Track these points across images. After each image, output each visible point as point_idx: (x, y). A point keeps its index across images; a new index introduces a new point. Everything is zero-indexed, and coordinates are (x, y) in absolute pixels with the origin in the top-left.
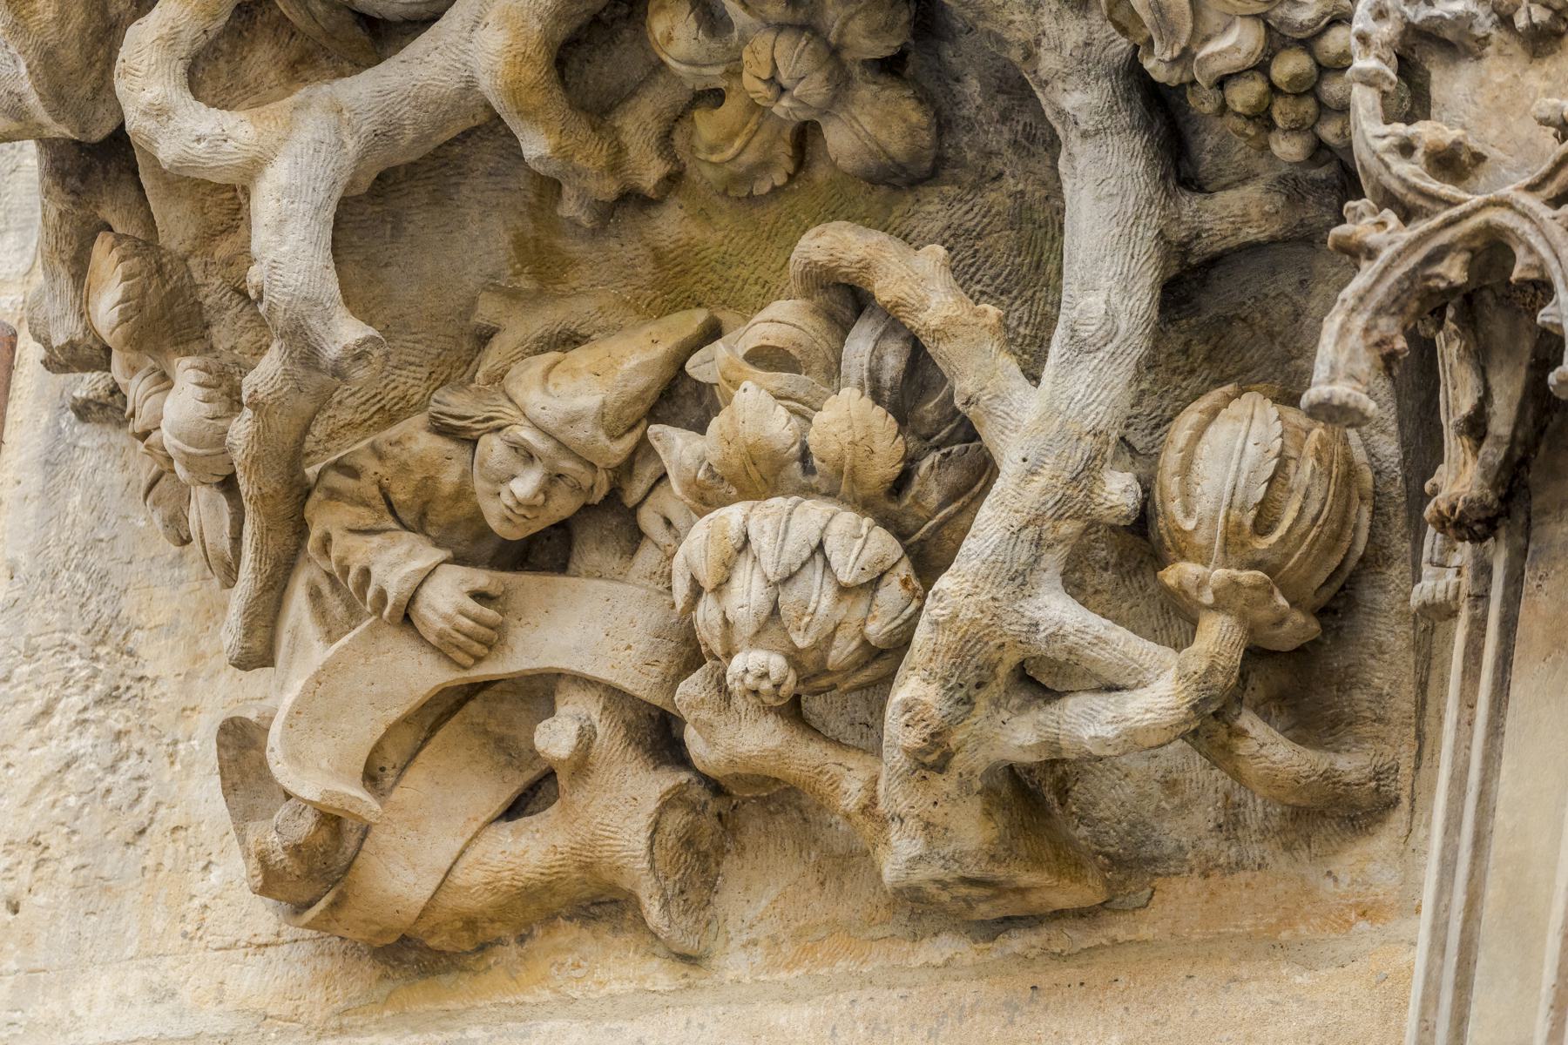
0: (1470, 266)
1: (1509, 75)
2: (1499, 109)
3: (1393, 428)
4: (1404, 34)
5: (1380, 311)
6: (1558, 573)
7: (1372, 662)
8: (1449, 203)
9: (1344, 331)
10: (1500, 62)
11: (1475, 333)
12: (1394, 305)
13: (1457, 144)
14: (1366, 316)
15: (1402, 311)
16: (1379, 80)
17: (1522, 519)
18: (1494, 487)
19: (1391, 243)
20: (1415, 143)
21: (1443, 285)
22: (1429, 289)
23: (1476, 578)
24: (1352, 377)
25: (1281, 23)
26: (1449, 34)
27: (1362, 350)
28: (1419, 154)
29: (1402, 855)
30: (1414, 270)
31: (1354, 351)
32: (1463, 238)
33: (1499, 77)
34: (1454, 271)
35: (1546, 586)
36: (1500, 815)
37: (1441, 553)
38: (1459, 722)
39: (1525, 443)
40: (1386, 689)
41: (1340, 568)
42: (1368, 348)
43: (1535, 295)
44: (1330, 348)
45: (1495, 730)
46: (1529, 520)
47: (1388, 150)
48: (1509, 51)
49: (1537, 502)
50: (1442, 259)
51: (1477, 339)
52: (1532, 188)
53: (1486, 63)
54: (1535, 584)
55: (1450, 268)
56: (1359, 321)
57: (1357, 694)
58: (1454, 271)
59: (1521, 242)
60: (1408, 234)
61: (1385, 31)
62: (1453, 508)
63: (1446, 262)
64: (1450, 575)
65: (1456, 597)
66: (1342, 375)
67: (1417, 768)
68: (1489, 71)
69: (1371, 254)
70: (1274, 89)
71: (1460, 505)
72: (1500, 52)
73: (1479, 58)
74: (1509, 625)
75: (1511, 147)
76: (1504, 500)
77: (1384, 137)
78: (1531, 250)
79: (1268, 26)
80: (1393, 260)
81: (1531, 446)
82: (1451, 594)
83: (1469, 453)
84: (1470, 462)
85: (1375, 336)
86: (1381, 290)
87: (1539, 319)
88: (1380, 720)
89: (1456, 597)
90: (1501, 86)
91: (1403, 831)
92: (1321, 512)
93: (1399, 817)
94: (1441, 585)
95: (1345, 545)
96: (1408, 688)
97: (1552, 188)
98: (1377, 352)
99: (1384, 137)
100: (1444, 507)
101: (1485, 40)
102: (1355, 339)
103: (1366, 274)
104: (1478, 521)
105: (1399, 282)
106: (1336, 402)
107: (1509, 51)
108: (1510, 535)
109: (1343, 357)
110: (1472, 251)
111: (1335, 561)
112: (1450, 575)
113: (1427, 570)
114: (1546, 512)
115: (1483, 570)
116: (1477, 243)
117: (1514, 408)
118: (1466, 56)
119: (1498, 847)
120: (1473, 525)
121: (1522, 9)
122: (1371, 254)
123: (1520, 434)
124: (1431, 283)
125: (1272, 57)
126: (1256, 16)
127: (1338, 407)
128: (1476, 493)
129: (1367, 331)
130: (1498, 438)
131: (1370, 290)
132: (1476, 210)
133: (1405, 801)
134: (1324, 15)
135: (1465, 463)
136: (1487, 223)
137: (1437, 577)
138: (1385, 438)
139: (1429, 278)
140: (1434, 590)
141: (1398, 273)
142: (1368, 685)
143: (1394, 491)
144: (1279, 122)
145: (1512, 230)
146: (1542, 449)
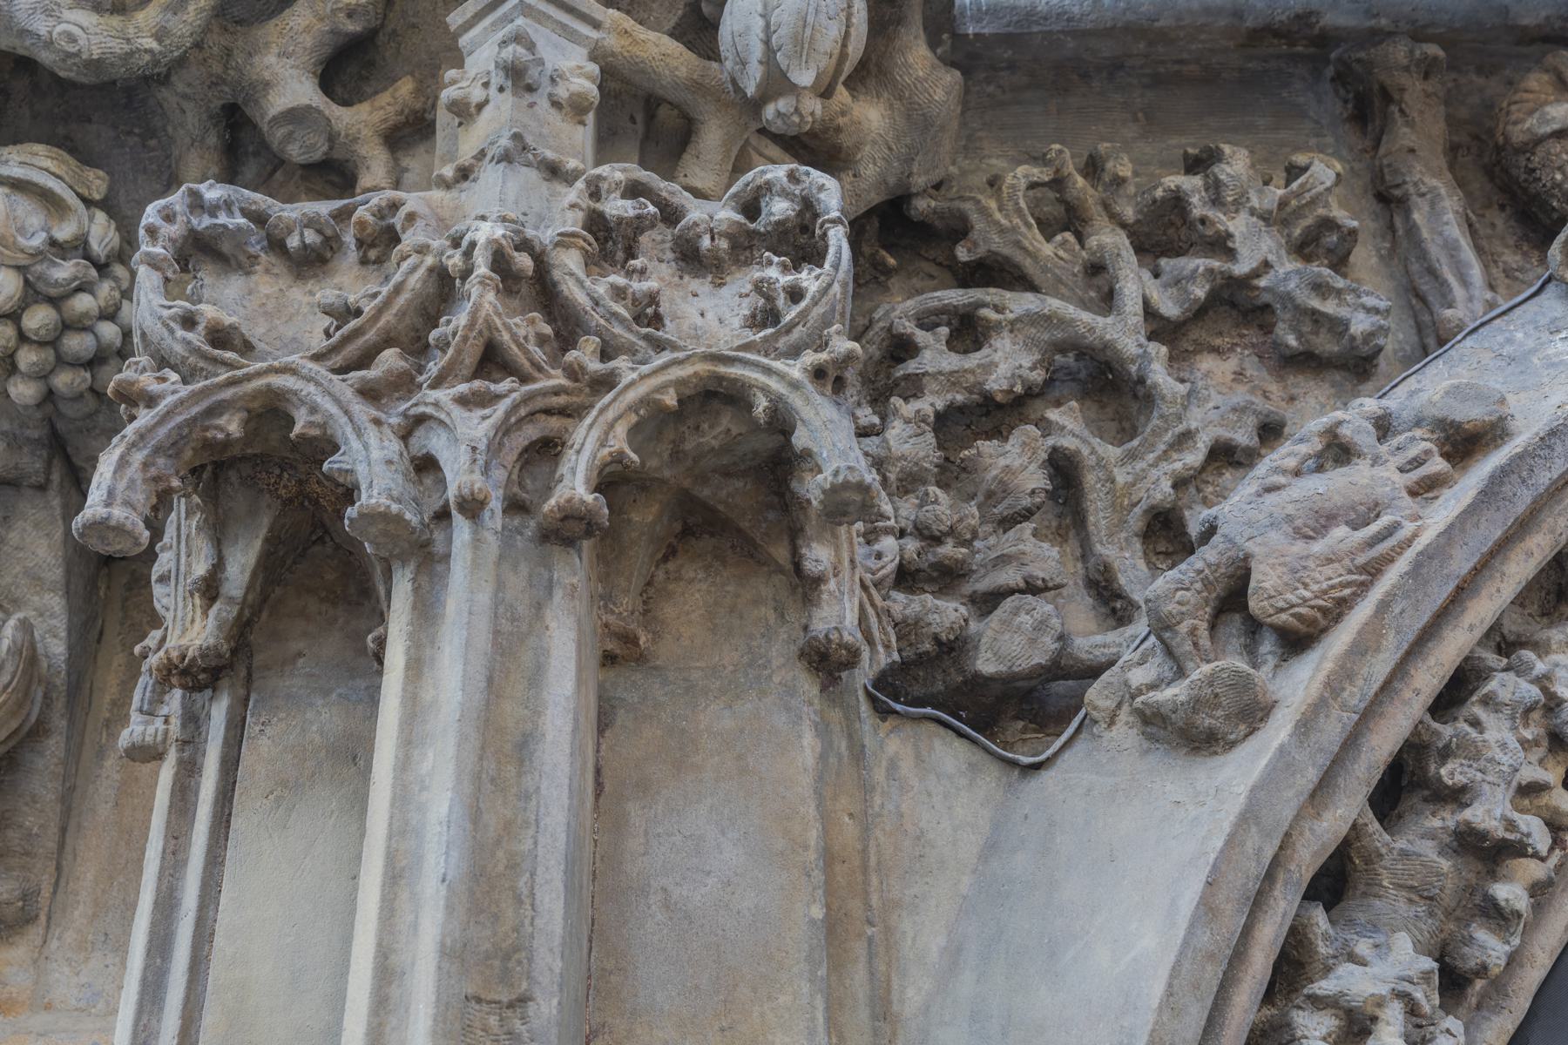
0: (246, 423)
1: (276, 288)
2: (266, 313)
3: (63, 634)
4: (185, 238)
5: (157, 450)
6: (280, 720)
7: (25, 809)
8: (231, 366)
9: (123, 463)
10: (267, 278)
11: (216, 506)
12: (172, 449)
13: (233, 327)
14: (145, 452)
15: (177, 455)
16: (165, 265)
17: (243, 673)
18: (228, 639)
19: (174, 392)
20: (198, 318)
21: (220, 436)
22: (205, 439)
23: (184, 726)
24: (127, 503)
25: (39, 278)
26: (226, 247)
27: (139, 482)
28: (200, 328)
29: (35, 962)
30: (194, 419)
31: (132, 481)
32: (241, 398)
33: (265, 289)
34: (232, 425)
35: (268, 730)
36: (219, 941)
37: (150, 703)
38: (164, 851)
39: (251, 607)
40: (35, 830)
41: (15, 732)
42: (145, 481)
43: (280, 476)
44: (108, 475)
45: (215, 860)
46: (249, 675)
47: (172, 318)
48: (276, 271)
49: (258, 659)
50: (221, 415)
51: (216, 513)
52: (317, 357)
53: (254, 278)
54: (257, 728)
55: (229, 422)
56: (138, 457)
57: (10, 833)
58: (232, 425)
59: (303, 403)
60: (185, 391)
61: (174, 230)
62: (183, 657)
63: (225, 417)
64: (159, 723)
65: (165, 740)
66: (119, 501)
67: (55, 892)
68: (257, 284)
69: (151, 401)
70: (23, 338)
71: (190, 654)
72: (267, 271)
73: (248, 274)
74: (230, 764)
75: (278, 343)
76: (234, 652)
77: (170, 307)
78: (314, 409)
79: (26, 281)
80: (176, 407)
81: (257, 610)
82: (159, 738)
83: (199, 611)
84: (198, 620)
85: (153, 471)
86: (162, 431)
87: (326, 466)
88: (27, 854)
89: (165, 740)
90: (267, 296)
91: (39, 941)
92: (10, 683)
93: (35, 933)
94: (151, 730)
95: (24, 712)
96: (53, 830)
97: (337, 360)
98: (153, 487)
99: (170, 307)
100: (174, 654)
101: (254, 258)
102: (134, 470)
103: (145, 417)
104: (204, 670)
105: (179, 427)
106: (113, 523)
107: (276, 271)
108: (232, 686)
109: (121, 485)
110: (249, 411)
111: (14, 725)
112: (159, 723)
113: (135, 717)
114: (267, 668)
115: (193, 720)
116: (256, 405)
117: (247, 575)
118: (235, 270)
119: (217, 972)
120: (199, 676)
121: (297, 232)
122: (151, 401)
123: (250, 597)
124: (209, 435)
125: (23, 310)
126: (18, 268)
127: (114, 529)
128: (212, 641)
129: (146, 465)
130: (231, 600)
131: (151, 429)
132: (259, 374)
133: (43, 918)
134: (75, 278)
135: (193, 621)
136: (269, 385)
137: (147, 723)
138: (56, 641)
139: (207, 429)
140: (144, 734)
141: (179, 419)
142: (21, 826)
143: (58, 682)
144: (22, 366)
145: (295, 393)
146: (264, 615)
